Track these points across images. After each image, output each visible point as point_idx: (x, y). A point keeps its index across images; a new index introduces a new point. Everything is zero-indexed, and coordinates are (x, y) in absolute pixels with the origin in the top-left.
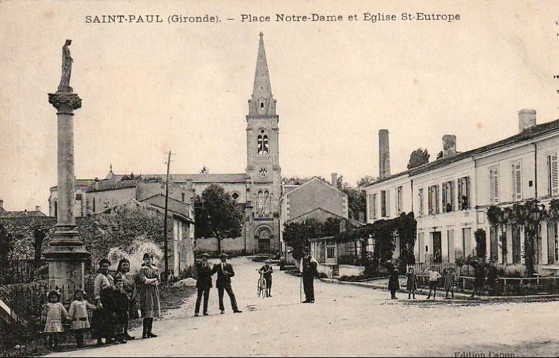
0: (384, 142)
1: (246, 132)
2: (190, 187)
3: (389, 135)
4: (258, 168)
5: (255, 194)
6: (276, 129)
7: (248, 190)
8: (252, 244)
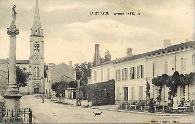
0: (97, 49)
1: (29, 42)
2: (6, 65)
3: (100, 46)
4: (34, 58)
5: (33, 69)
6: (43, 42)
7: (30, 67)
8: (31, 90)
